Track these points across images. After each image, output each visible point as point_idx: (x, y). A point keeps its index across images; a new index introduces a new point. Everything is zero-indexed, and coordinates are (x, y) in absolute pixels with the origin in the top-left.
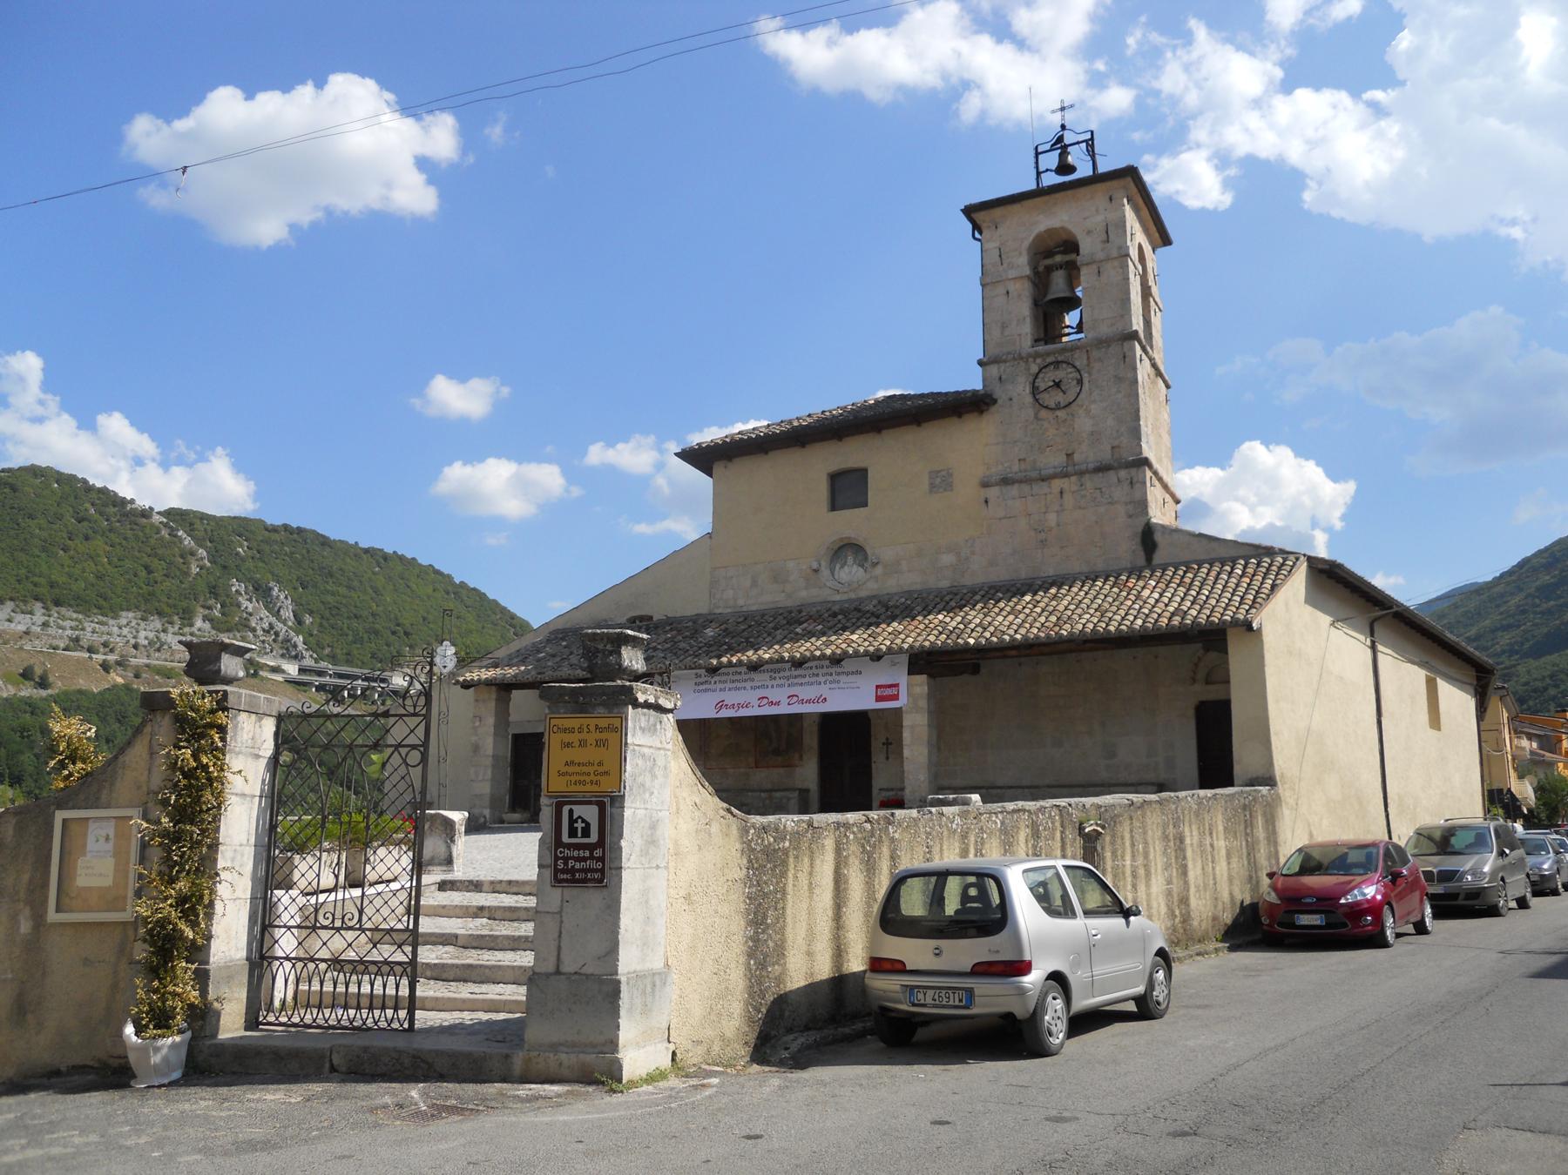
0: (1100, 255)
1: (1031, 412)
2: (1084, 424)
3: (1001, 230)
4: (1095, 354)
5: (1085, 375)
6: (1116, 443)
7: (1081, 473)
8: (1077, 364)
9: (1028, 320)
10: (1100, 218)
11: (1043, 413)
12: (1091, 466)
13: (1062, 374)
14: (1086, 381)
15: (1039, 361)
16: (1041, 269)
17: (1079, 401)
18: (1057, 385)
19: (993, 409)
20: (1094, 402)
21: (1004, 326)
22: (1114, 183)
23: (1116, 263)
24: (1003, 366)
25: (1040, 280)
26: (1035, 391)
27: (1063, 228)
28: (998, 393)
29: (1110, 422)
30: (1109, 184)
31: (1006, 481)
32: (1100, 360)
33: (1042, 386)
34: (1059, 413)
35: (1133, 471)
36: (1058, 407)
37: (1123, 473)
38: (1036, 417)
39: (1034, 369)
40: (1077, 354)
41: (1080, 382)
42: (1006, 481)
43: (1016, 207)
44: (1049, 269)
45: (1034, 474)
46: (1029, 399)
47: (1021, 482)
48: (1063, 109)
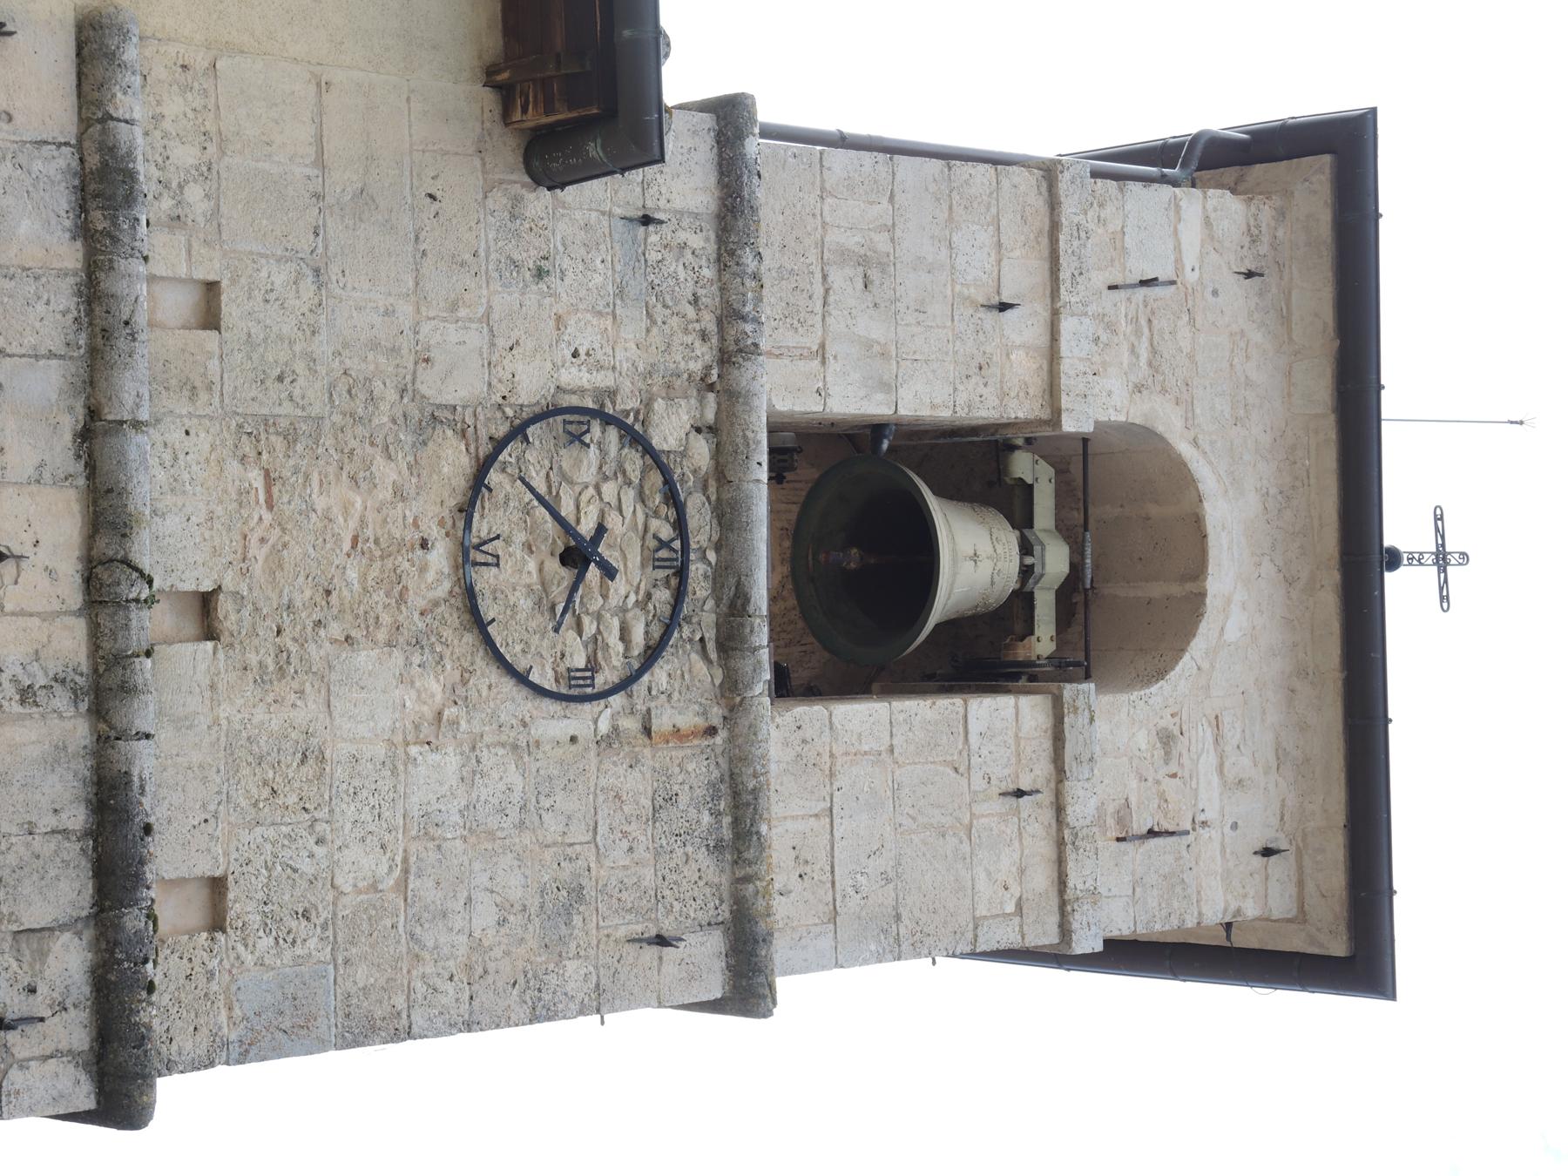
0: (1081, 809)
1: (459, 384)
2: (376, 698)
3: (1237, 295)
4: (695, 770)
5: (605, 716)
6: (239, 904)
7: (106, 687)
8: (659, 675)
9: (876, 407)
10: (1211, 799)
11: (454, 461)
12: (144, 761)
13: (626, 592)
14: (584, 721)
15: (701, 452)
16: (1023, 465)
17: (487, 676)
18: (578, 555)
19: (507, 151)
20: (472, 775)
21: (871, 269)
22: (1334, 878)
23: (1041, 879)
24: (702, 241)
25: (976, 462)
26: (572, 419)
27: (1195, 604)
28: (596, 200)
29: (360, 864)
30: (1335, 848)
31: (102, 190)
32: (664, 800)
33: (586, 464)
34: (439, 558)
35: (74, 1031)
36: (468, 555)
37: (70, 961)
38: (435, 419)
39: (671, 428)
40: (705, 674)
41: (577, 690)
42: (102, 190)
43: (1318, 386)
44: (1015, 506)
45: (132, 390)
46: (531, 388)
47: (93, 293)
48: (1441, 559)
